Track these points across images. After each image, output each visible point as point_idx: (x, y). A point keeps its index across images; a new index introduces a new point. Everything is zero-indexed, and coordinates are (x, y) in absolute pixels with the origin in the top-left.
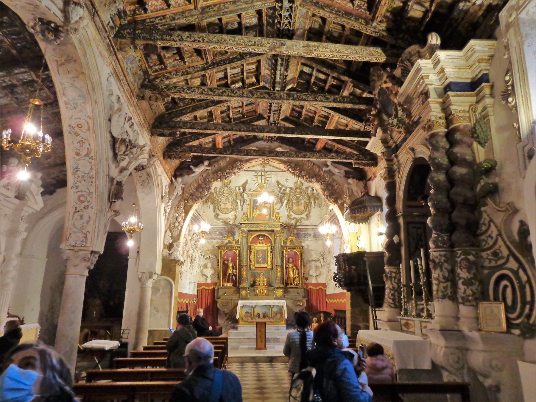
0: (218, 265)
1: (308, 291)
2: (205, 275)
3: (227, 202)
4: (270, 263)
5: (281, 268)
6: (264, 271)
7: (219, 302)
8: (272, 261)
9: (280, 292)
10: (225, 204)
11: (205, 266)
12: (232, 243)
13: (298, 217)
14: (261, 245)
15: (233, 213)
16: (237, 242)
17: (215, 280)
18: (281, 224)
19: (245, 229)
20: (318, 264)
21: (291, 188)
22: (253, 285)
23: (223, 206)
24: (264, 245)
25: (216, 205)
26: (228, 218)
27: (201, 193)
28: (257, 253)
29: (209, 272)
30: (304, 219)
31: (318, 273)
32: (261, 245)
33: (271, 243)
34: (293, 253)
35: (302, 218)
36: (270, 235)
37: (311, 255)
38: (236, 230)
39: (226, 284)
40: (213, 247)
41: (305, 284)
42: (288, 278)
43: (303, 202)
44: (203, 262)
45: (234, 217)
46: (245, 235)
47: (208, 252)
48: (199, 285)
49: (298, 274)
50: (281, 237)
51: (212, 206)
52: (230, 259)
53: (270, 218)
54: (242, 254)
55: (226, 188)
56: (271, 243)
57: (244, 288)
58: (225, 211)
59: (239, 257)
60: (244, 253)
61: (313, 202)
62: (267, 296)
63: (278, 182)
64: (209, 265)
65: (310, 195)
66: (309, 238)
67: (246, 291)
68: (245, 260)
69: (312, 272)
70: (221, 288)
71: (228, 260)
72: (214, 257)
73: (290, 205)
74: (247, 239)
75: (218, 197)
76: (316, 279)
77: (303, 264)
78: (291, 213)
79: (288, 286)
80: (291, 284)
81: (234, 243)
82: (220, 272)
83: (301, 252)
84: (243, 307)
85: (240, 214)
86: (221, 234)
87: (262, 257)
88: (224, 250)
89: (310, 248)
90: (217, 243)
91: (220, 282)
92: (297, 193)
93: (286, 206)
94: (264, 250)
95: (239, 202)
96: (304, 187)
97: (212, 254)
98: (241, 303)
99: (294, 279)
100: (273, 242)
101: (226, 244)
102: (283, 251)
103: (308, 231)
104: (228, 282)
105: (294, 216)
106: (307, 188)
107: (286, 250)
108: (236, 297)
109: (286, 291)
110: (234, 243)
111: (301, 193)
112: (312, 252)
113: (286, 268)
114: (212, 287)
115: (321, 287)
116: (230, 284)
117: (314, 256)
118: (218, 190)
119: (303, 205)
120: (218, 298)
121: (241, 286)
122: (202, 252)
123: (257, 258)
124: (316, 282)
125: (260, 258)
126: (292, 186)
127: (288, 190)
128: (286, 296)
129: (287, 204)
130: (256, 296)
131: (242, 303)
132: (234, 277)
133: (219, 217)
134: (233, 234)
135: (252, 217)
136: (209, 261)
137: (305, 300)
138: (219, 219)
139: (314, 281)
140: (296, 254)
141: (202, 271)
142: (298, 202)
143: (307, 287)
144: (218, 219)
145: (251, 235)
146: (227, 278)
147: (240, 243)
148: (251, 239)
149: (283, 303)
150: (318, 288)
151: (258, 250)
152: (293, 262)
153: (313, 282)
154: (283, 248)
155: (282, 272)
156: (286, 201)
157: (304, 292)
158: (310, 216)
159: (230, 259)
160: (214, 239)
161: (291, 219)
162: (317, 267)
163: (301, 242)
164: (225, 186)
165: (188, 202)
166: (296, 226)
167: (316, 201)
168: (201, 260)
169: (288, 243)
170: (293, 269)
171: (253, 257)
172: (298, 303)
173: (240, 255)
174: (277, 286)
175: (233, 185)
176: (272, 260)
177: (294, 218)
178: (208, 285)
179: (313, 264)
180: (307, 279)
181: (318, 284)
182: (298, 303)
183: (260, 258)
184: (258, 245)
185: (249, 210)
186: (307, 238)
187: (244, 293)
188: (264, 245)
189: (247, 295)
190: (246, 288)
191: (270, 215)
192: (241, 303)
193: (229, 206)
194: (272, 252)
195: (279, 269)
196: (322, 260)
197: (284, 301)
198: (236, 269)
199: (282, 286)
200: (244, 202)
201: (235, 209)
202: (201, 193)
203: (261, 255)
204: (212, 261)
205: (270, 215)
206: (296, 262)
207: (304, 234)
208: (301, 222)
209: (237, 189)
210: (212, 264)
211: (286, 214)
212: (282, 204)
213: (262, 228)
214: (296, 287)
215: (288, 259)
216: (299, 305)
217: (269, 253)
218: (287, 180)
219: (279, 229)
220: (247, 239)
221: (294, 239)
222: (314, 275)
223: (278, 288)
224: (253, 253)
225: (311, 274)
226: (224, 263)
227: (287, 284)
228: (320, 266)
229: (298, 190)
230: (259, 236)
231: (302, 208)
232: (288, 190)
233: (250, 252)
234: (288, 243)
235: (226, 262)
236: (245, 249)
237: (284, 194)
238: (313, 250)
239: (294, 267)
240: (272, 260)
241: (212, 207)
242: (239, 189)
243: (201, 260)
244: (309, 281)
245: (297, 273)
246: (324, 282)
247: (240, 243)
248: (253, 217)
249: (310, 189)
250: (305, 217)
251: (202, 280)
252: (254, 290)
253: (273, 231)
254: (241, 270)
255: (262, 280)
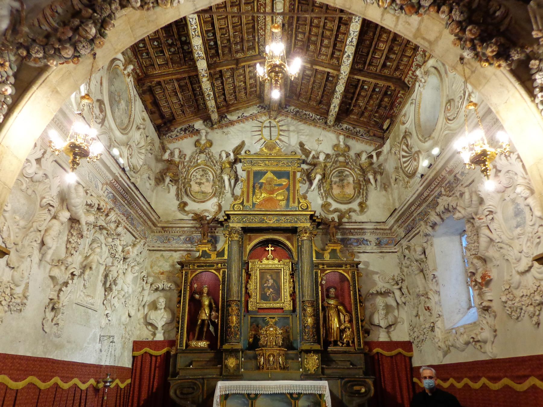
0: (179, 302)
1: (373, 357)
2: (151, 324)
3: (204, 180)
4: (289, 298)
5: (312, 306)
6: (277, 316)
7: (174, 383)
8: (293, 295)
9: (312, 362)
10: (200, 184)
11: (154, 306)
12: (209, 256)
13: (344, 207)
14: (270, 262)
15: (215, 200)
16: (221, 254)
17: (173, 336)
18: (312, 216)
19: (238, 226)
20: (390, 301)
21: (328, 156)
22: (254, 344)
23: (195, 188)
24: (276, 261)
25: (181, 186)
26: (206, 211)
27: (76, 30)
28: (262, 278)
29: (161, 318)
30: (354, 211)
31: (391, 319)
32: (271, 262)
33: (291, 257)
34: (337, 278)
35: (351, 210)
36: (288, 239)
37: (375, 284)
38: (220, 233)
39: (193, 344)
40: (173, 266)
41: (366, 343)
42: (328, 329)
43: (351, 179)
44: (148, 297)
45: (216, 208)
46: (236, 237)
47: (162, 277)
48: (137, 345)
49: (350, 321)
50: (309, 246)
51: (175, 187)
52: (205, 290)
53: (287, 205)
54: (229, 276)
55: (203, 156)
56: (291, 257)
57: (233, 352)
58: (200, 197)
59: (223, 284)
60: (234, 275)
61: (371, 177)
62: (285, 372)
63: (302, 145)
64: (162, 302)
65: (365, 166)
66: (368, 249)
67: (237, 358)
68: (235, 289)
69: (379, 319)
70: (183, 352)
71: (201, 293)
72: (173, 287)
73: (326, 185)
74: (241, 247)
75: (188, 171)
76: (388, 332)
77: (362, 299)
78: (330, 200)
79: (330, 348)
80: (335, 344)
81: (214, 257)
82: (183, 316)
83: (353, 274)
84: (226, 397)
85: (227, 202)
86: (190, 240)
87: (274, 283)
88: (194, 271)
89: (371, 268)
90: (182, 257)
91: (182, 338)
92: (338, 164)
93: (319, 188)
94: (276, 273)
95: (226, 178)
96: (352, 153)
97: (169, 280)
98: (222, 387)
99: (342, 331)
100: (295, 255)
101: (199, 257)
102: (316, 273)
103: (364, 233)
104: (199, 339)
105: (335, 205)
106: (358, 155)
107: (323, 271)
108: (214, 372)
109: (326, 359)
110: (214, 257)
111: (347, 163)
112: (376, 277)
113: (324, 308)
114: (164, 350)
115: (400, 350)
116: (203, 344)
117: (381, 285)
118: (187, 159)
119: (352, 186)
120: (175, 374)
121: (226, 346)
122: (149, 275)
123: (262, 288)
124: (387, 340)
125: (269, 288)
126: (330, 151)
127: (322, 157)
128: (327, 372)
129: (321, 181)
130: (260, 372)
131: (226, 388)
132: (211, 328)
133: (187, 209)
134: (214, 241)
135: (251, 203)
136: (162, 294)
137: (370, 382)
138: (187, 213)
139: (383, 337)
140: (343, 278)
141: (145, 317)
142: (342, 180)
143: (371, 350)
144: (185, 211)
145: (250, 240)
146: (197, 329)
147: (226, 257)
148: (249, 248)
149: (323, 386)
150: (394, 353)
151: (263, 272)
152: (336, 297)
153: (381, 340)
154: (317, 265)
155: (316, 316)
156: (318, 177)
157: (366, 363)
158: (366, 206)
159: (205, 290)
160: (175, 251)
161: (329, 211)
162: (388, 308)
163: (353, 254)
164: (201, 152)
165: (29, 55)
166: (340, 223)
167: (379, 177)
168: (146, 293)
169: (327, 256)
170: (339, 311)
171: (254, 286)
172: (356, 388)
173: (226, 281)
174: (306, 346)
175: (215, 150)
176: (294, 292)
177: (336, 210)
178: (155, 345)
179: (380, 301)
180: (367, 332)
181: (391, 345)
182: (356, 388)
183: (269, 288)
184: (265, 261)
185: (245, 190)
186: (362, 248)
187: (231, 362)
188: (276, 261)
189: (238, 367)
190: (236, 351)
191: (288, 200)
192: (222, 387)
193: (208, 188)
194: (292, 275)
195: (309, 310)
196: (397, 293)
197: (325, 383)
198: (217, 311)
199: (317, 347)
200: (237, 180)
201: (218, 193)
202: (76, 30)
203: (271, 281)
204: (169, 294)
205: (288, 200)
206: (343, 296)
207: (358, 240)
208: (350, 217)
209: (224, 155)
210: (169, 301)
211: (320, 202)
212: (311, 184)
213: (271, 223)
214: (347, 349)
215: (328, 290)
216: (358, 392)
217: (288, 277)
218: (319, 141)
219: (308, 225)
220: (241, 247)
221: (338, 248)
222: (383, 324)
223: (308, 352)
224: (253, 277)
225: (376, 322)
226: (192, 299)
227: (327, 343)
228: (394, 304)
229: (341, 159)
230: (265, 243)
231: (350, 191)
232: (322, 157)
233: (249, 276)
234: (327, 256)
235: (197, 296)
236: (235, 267)
237: (315, 165)
238: (377, 273)
239: (341, 308)
240: (294, 292)
241: (173, 189)
242: (228, 155)
243: (146, 293)
244: (373, 337)
245: (347, 319)
246: (407, 339)
247: (226, 257)
248: (254, 205)
249: (364, 157)
250: (357, 208)
251: (145, 334)
252: (255, 358)
253: (294, 231)
254: (228, 310)
255: (272, 333)
